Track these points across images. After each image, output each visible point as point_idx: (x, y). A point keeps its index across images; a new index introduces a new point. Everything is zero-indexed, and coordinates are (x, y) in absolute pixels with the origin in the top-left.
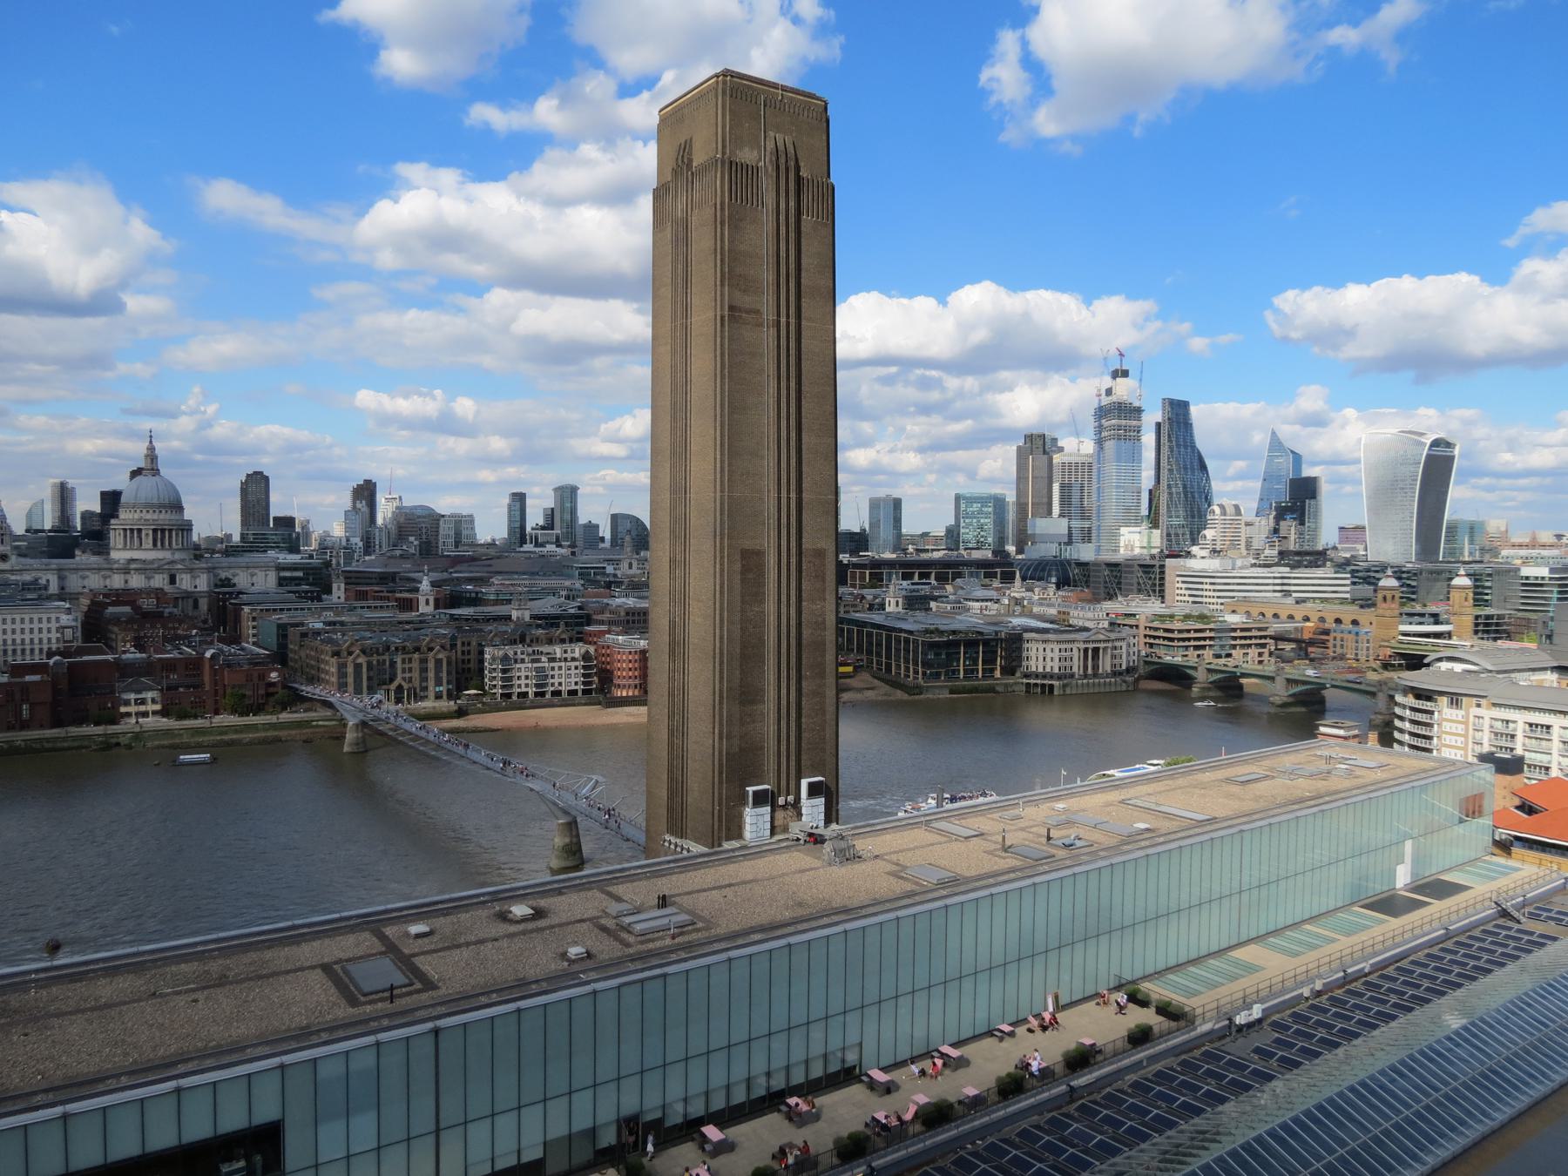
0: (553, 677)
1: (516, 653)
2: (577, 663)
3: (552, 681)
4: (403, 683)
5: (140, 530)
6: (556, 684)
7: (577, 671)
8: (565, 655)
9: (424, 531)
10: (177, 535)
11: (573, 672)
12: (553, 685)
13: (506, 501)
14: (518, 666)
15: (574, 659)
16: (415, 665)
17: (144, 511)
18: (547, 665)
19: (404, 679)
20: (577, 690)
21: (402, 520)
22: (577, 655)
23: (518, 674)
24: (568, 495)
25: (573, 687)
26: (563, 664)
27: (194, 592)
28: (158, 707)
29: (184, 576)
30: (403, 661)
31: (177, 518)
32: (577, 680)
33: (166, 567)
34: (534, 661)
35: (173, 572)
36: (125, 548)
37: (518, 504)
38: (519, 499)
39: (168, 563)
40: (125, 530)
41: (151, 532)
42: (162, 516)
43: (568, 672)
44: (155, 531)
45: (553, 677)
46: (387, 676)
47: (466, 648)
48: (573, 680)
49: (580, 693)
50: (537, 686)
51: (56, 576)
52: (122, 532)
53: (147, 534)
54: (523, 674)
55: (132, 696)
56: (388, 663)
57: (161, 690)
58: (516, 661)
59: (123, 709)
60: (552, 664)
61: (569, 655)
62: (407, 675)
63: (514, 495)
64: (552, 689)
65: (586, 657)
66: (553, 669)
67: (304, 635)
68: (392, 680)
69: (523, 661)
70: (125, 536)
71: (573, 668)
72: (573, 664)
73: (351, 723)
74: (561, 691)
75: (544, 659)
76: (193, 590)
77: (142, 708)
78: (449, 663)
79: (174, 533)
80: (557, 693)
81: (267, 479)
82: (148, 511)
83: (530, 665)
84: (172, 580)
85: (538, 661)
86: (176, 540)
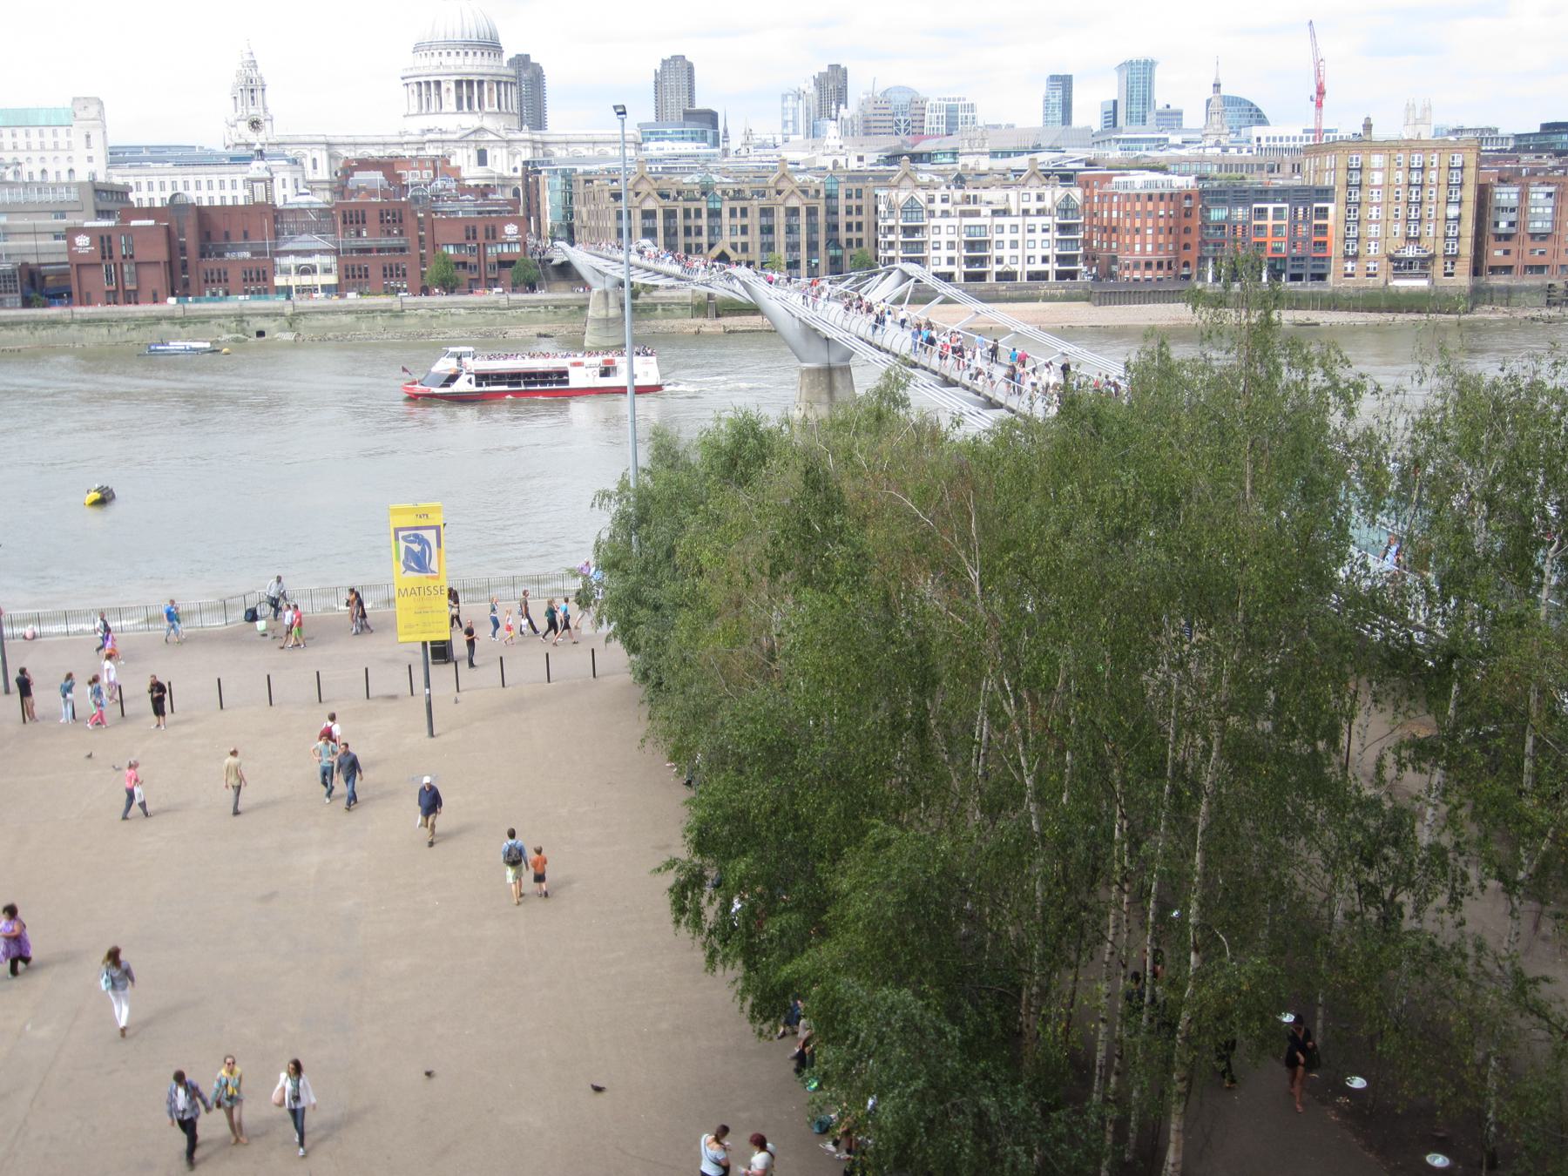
0: (1000, 244)
1: (931, 201)
2: (1047, 220)
3: (997, 253)
4: (729, 252)
5: (438, 83)
6: (1006, 261)
7: (1047, 236)
8: (1024, 206)
9: (902, 126)
10: (490, 90)
11: (1039, 236)
12: (999, 261)
13: (1041, 89)
14: (934, 222)
15: (1040, 212)
16: (754, 221)
17: (444, 53)
18: (987, 221)
19: (734, 246)
20: (1047, 272)
21: (870, 111)
22: (1047, 203)
23: (934, 238)
24: (1139, 75)
25: (1039, 266)
26: (1019, 221)
27: (511, 178)
28: (332, 279)
29: (497, 152)
30: (733, 212)
31: (497, 64)
32: (1047, 252)
33: (472, 137)
34: (963, 214)
35: (482, 146)
36: (419, 114)
37: (1059, 93)
38: (1063, 84)
39: (475, 132)
40: (419, 84)
41: (453, 86)
42: (470, 59)
43: (1030, 236)
44: (459, 83)
45: (1000, 244)
46: (704, 240)
47: (854, 202)
48: (1039, 253)
49: (1052, 278)
50: (970, 261)
51: (325, 154)
52: (415, 87)
53: (448, 89)
54: (944, 238)
55: (290, 261)
56: (705, 215)
57: (337, 252)
58: (932, 214)
59: (279, 281)
60: (999, 220)
61: (1034, 206)
62: (740, 239)
63: (1053, 78)
64: (999, 268)
65: (1065, 209)
66: (1001, 228)
67: (587, 181)
68: (711, 246)
69: (945, 213)
70: (420, 95)
71: (1039, 229)
72: (1040, 222)
73: (595, 290)
74: (1016, 273)
75: (986, 211)
76: (512, 174)
77: (307, 280)
78: (812, 212)
79: (485, 85)
80: (1007, 276)
81: (690, 68)
82: (449, 54)
83: (955, 221)
84: (482, 159)
85: (977, 214)
86: (490, 100)
